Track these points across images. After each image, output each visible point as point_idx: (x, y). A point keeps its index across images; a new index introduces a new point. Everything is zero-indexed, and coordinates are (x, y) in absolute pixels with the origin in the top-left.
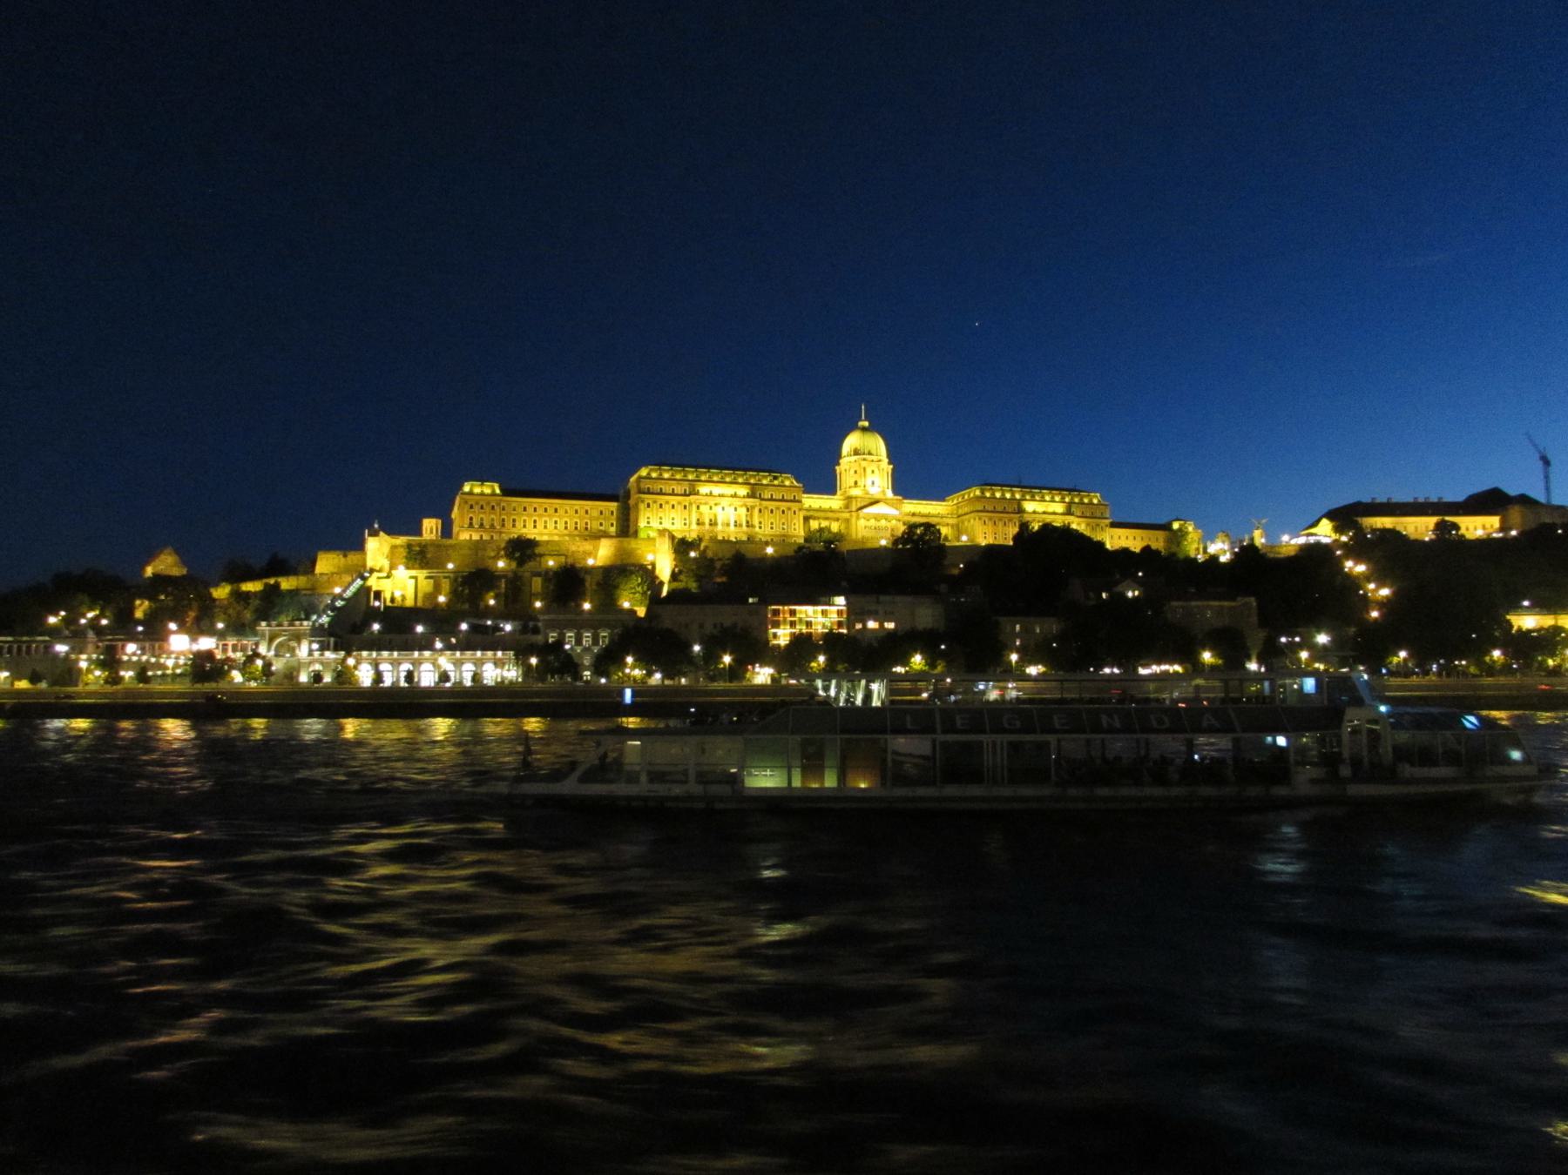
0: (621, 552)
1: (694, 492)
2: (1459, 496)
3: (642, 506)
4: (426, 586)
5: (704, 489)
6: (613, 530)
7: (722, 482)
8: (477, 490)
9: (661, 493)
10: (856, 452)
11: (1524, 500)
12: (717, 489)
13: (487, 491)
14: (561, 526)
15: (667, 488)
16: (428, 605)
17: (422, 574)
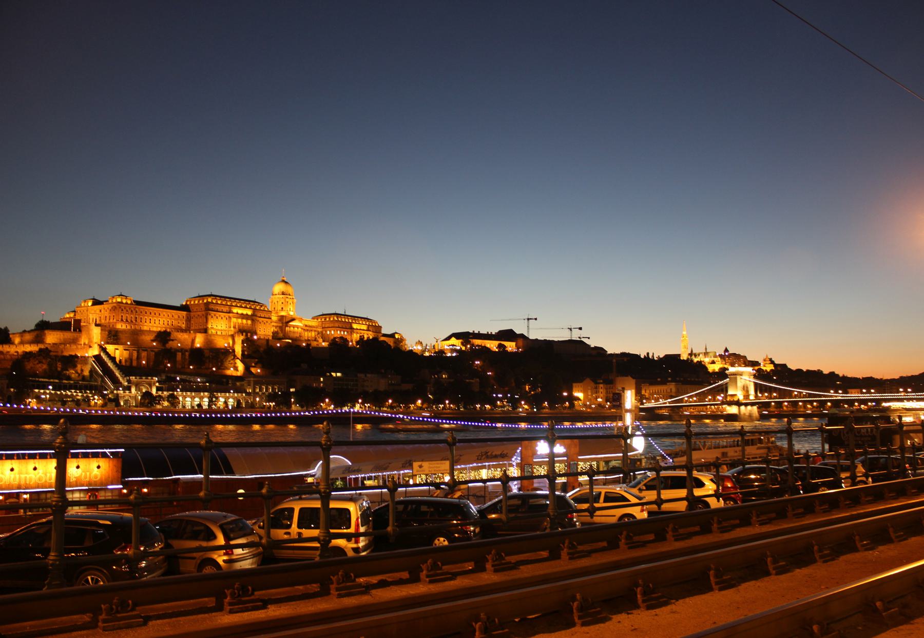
0: (208, 342)
1: (230, 312)
2: (494, 331)
3: (209, 317)
4: (126, 354)
5: (235, 310)
6: (184, 326)
7: (241, 307)
8: (124, 301)
9: (217, 311)
10: (283, 294)
11: (522, 336)
12: (240, 311)
13: (129, 302)
14: (161, 322)
15: (220, 308)
16: (128, 364)
17: (121, 347)
